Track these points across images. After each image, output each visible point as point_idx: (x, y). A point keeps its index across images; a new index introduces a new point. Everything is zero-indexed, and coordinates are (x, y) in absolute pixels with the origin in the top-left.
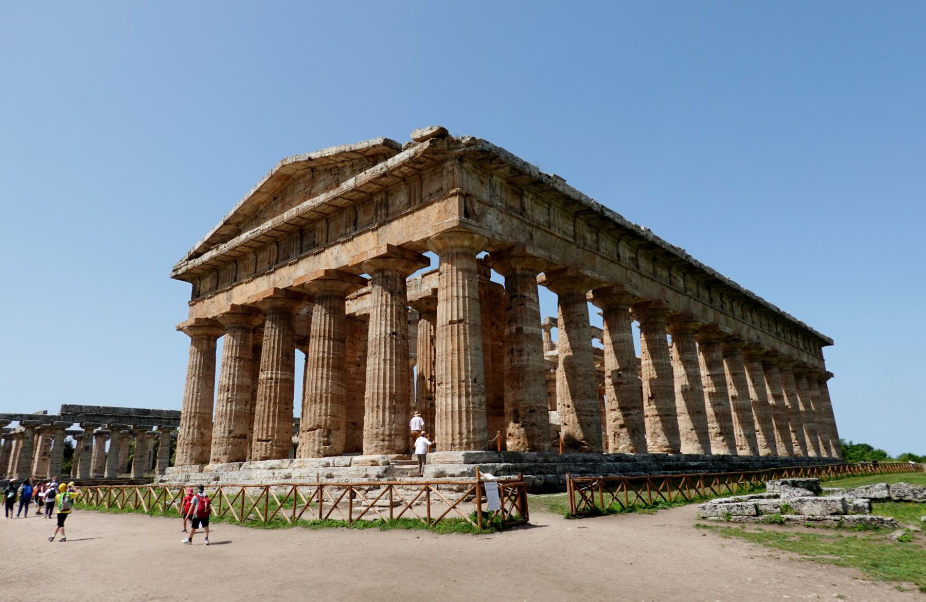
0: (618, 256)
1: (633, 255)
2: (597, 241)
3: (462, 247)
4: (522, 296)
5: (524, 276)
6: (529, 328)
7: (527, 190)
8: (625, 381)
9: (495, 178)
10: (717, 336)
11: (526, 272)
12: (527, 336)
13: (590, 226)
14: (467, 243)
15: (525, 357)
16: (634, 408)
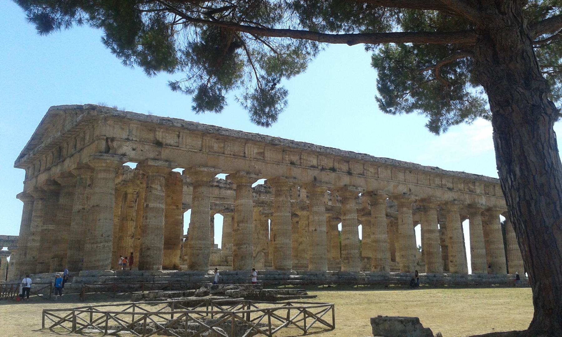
0: (245, 153)
1: (262, 151)
2: (224, 147)
3: (102, 166)
4: (151, 187)
5: (153, 176)
6: (152, 204)
7: (159, 128)
8: (240, 228)
9: (132, 125)
10: (350, 194)
11: (155, 174)
12: (151, 208)
13: (217, 139)
14: (104, 165)
15: (148, 220)
16: (245, 244)
